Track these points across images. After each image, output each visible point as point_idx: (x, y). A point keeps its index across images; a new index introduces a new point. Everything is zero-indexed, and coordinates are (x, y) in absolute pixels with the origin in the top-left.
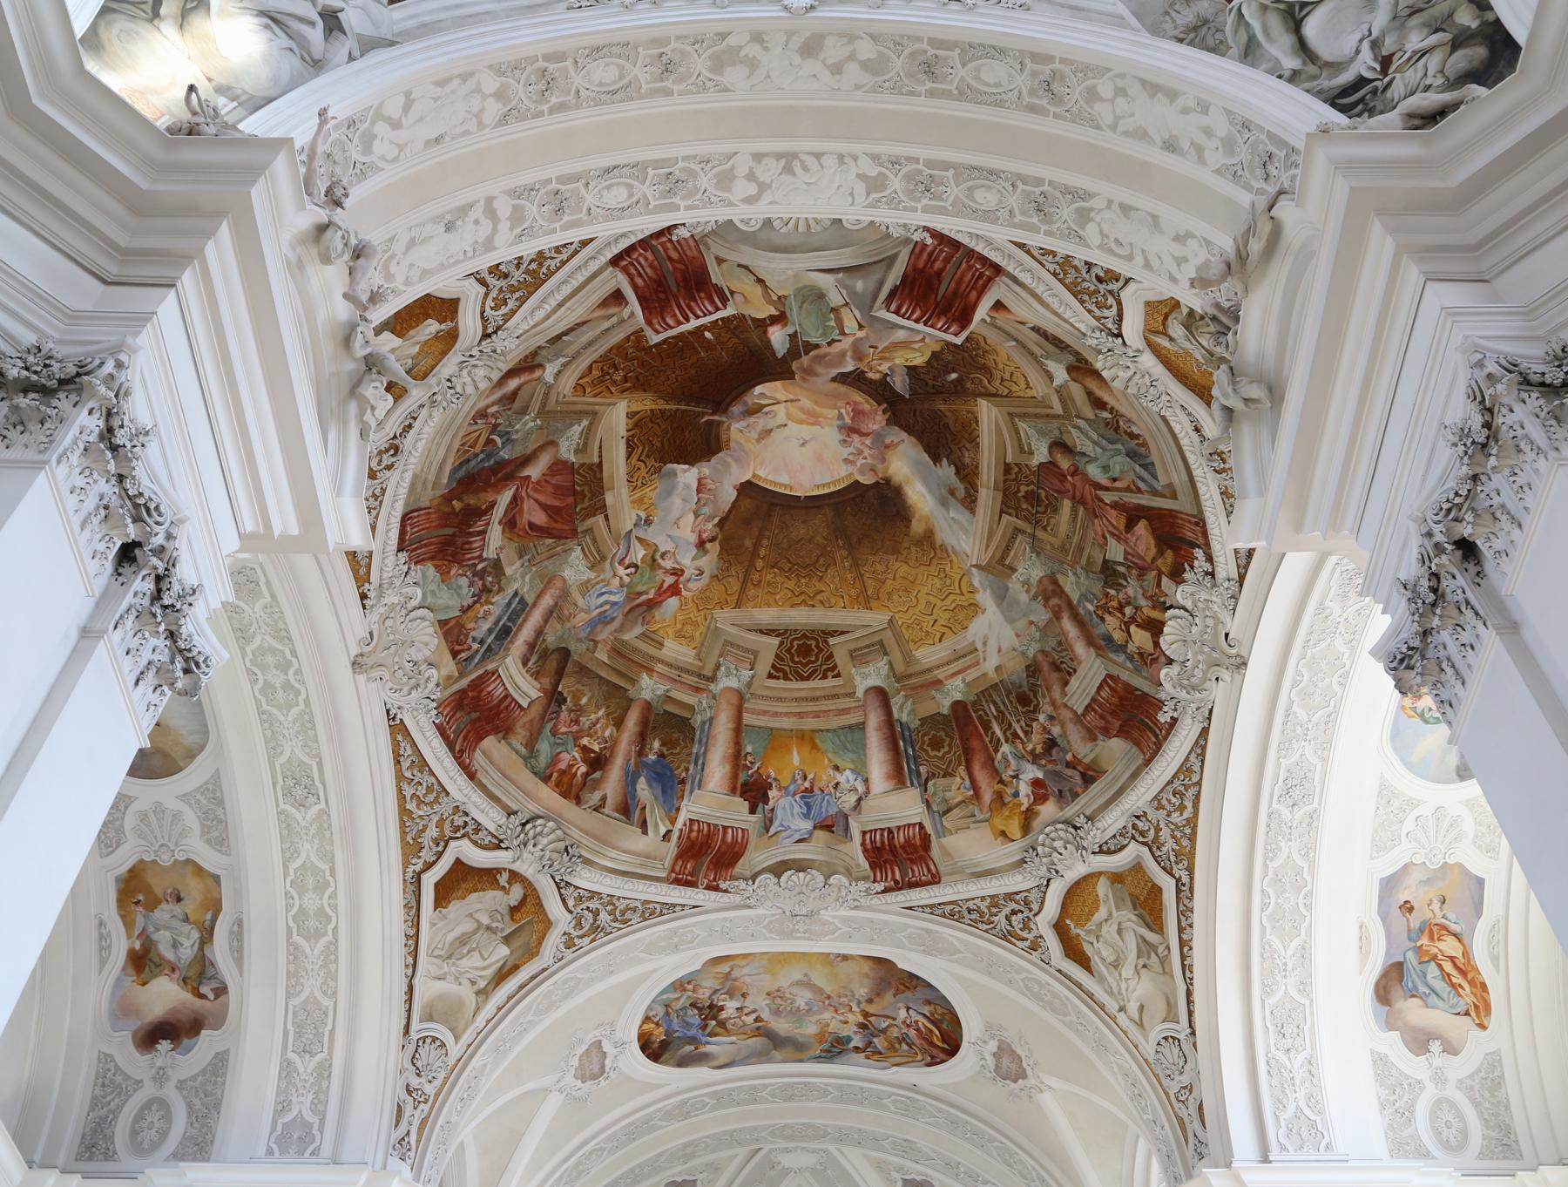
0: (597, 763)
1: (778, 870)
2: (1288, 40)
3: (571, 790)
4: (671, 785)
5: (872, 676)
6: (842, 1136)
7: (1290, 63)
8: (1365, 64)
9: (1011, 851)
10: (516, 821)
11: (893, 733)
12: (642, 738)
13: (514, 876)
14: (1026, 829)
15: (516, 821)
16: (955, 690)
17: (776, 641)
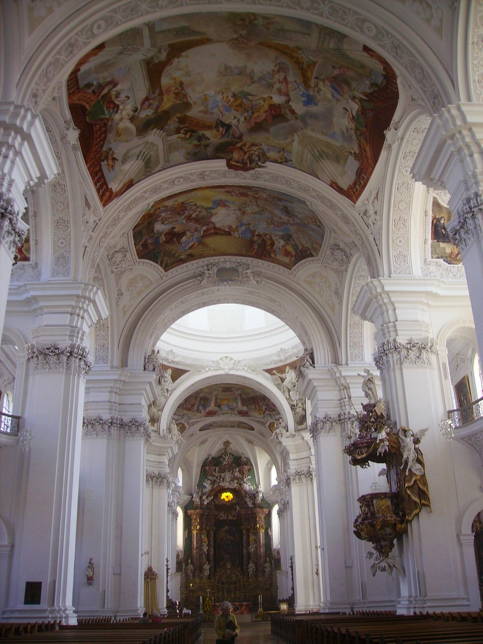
0: (193, 405)
1: (223, 414)
2: (288, 393)
3: (189, 410)
4: (205, 407)
5: (239, 392)
6: (234, 434)
7: (288, 397)
8: (295, 403)
9: (262, 416)
10: (180, 417)
11: (242, 399)
12: (200, 402)
13: (180, 423)
14: (264, 414)
15: (180, 417)
16: (253, 395)
17: (222, 389)
